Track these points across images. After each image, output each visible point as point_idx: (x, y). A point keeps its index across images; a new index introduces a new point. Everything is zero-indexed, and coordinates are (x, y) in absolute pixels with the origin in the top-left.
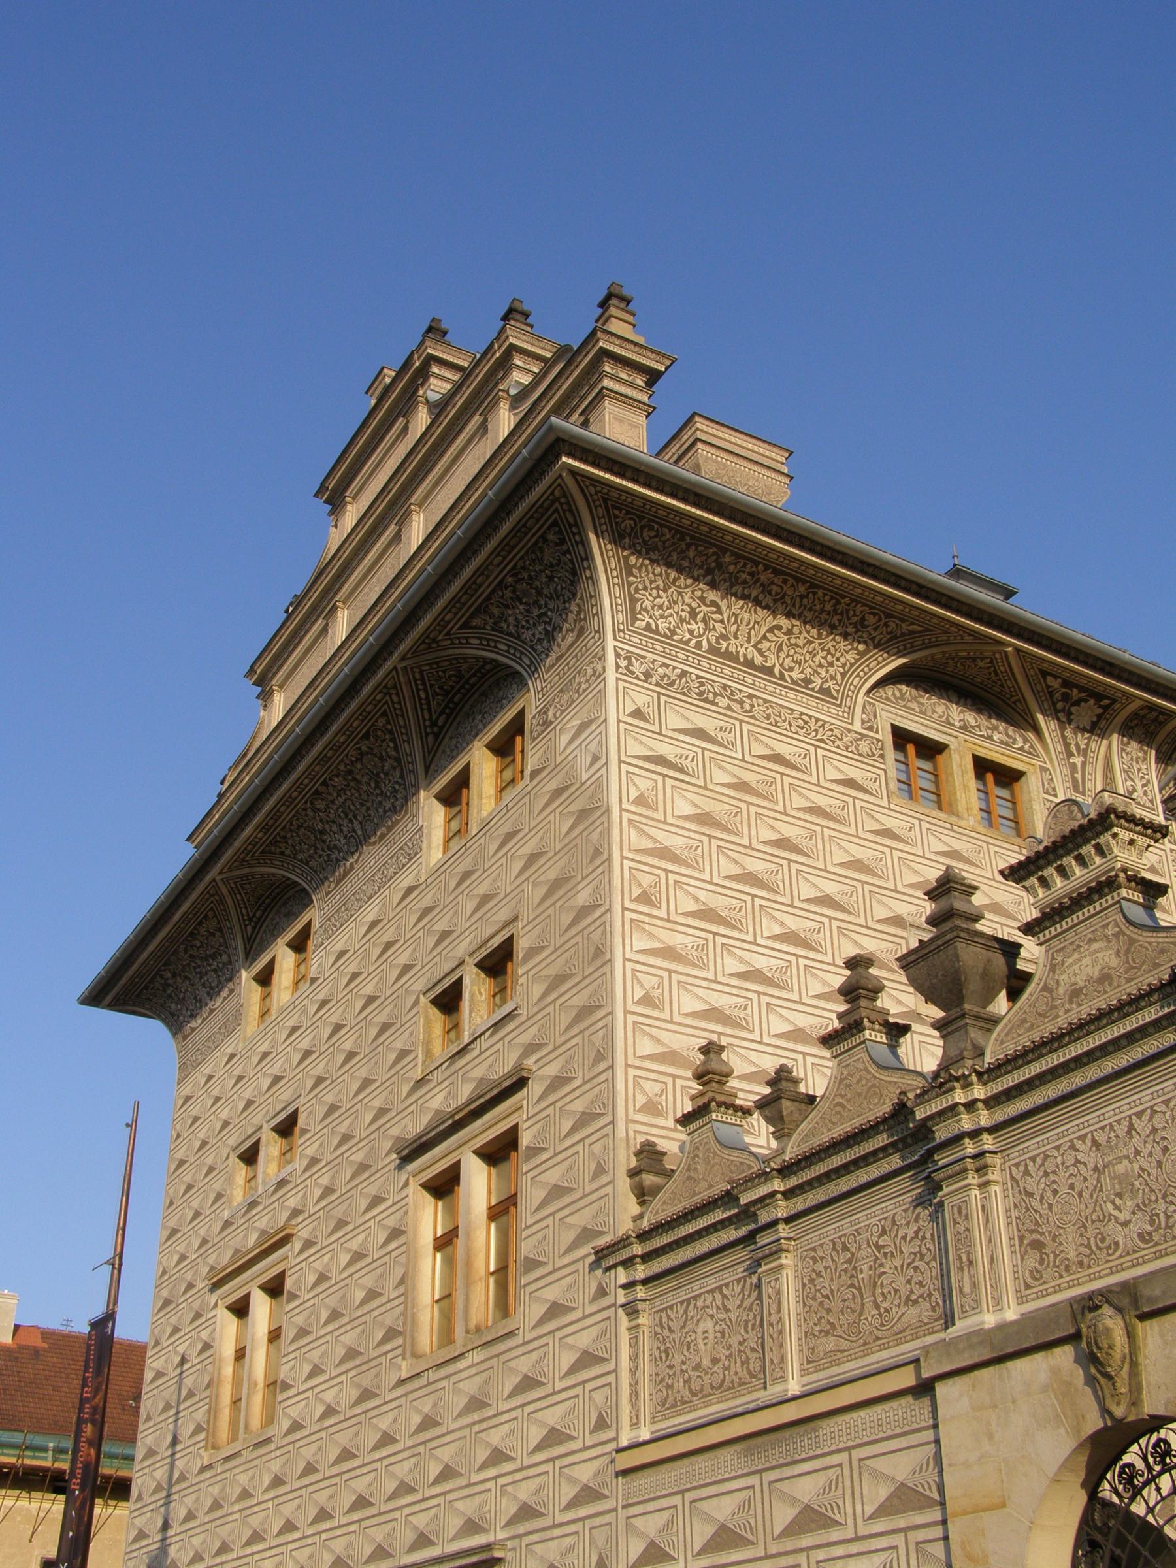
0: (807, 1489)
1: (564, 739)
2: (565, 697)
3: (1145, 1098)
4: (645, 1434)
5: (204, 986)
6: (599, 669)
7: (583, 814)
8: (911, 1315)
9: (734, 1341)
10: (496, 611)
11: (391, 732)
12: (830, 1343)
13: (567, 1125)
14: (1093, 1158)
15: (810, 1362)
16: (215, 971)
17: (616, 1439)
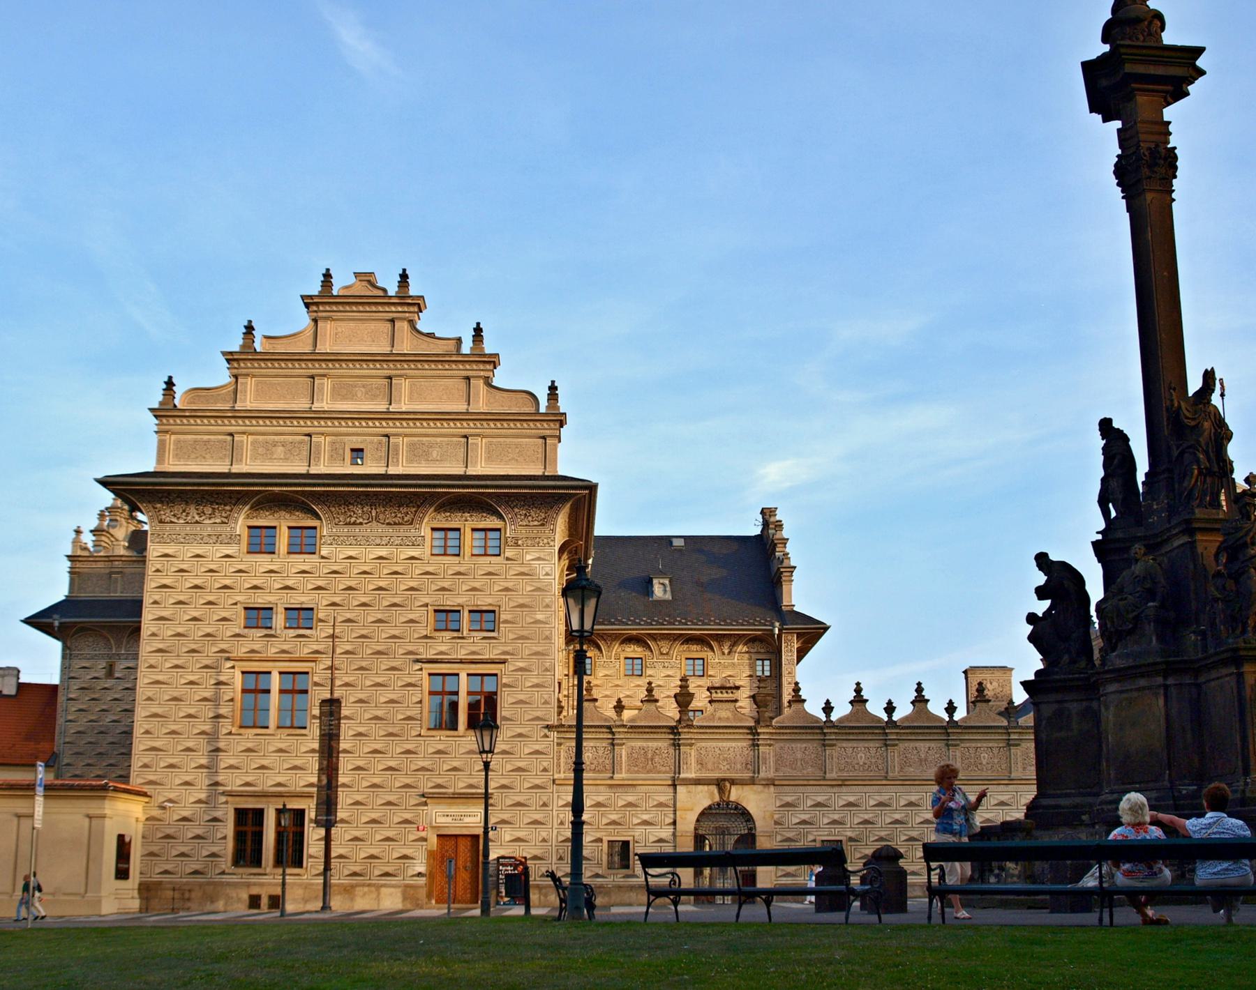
0: (631, 799)
1: (529, 557)
2: (529, 542)
3: (733, 744)
4: (562, 775)
5: (197, 509)
6: (552, 543)
7: (538, 589)
8: (663, 769)
9: (601, 761)
10: (512, 499)
11: (426, 499)
12: (636, 769)
13: (530, 684)
14: (719, 752)
15: (628, 771)
16: (214, 509)
17: (553, 775)
